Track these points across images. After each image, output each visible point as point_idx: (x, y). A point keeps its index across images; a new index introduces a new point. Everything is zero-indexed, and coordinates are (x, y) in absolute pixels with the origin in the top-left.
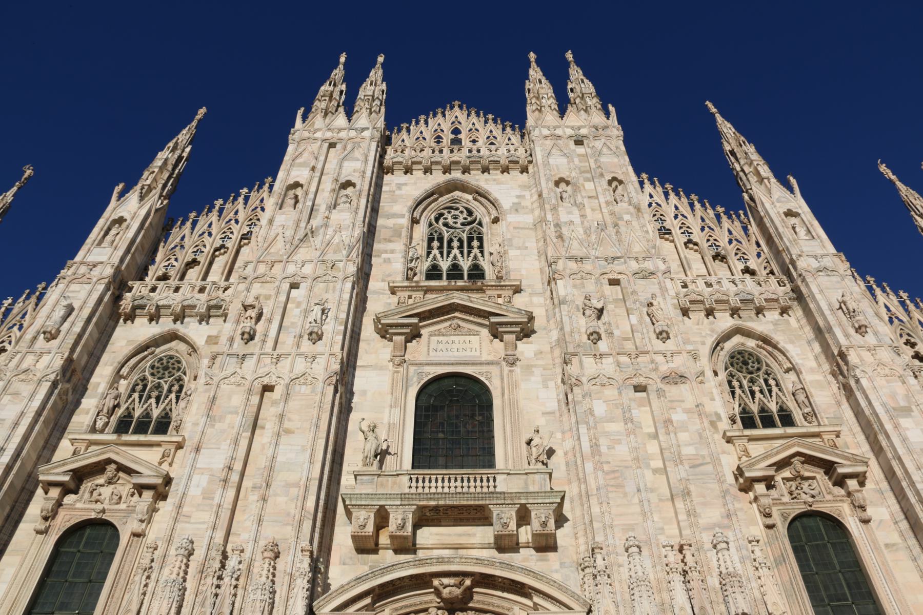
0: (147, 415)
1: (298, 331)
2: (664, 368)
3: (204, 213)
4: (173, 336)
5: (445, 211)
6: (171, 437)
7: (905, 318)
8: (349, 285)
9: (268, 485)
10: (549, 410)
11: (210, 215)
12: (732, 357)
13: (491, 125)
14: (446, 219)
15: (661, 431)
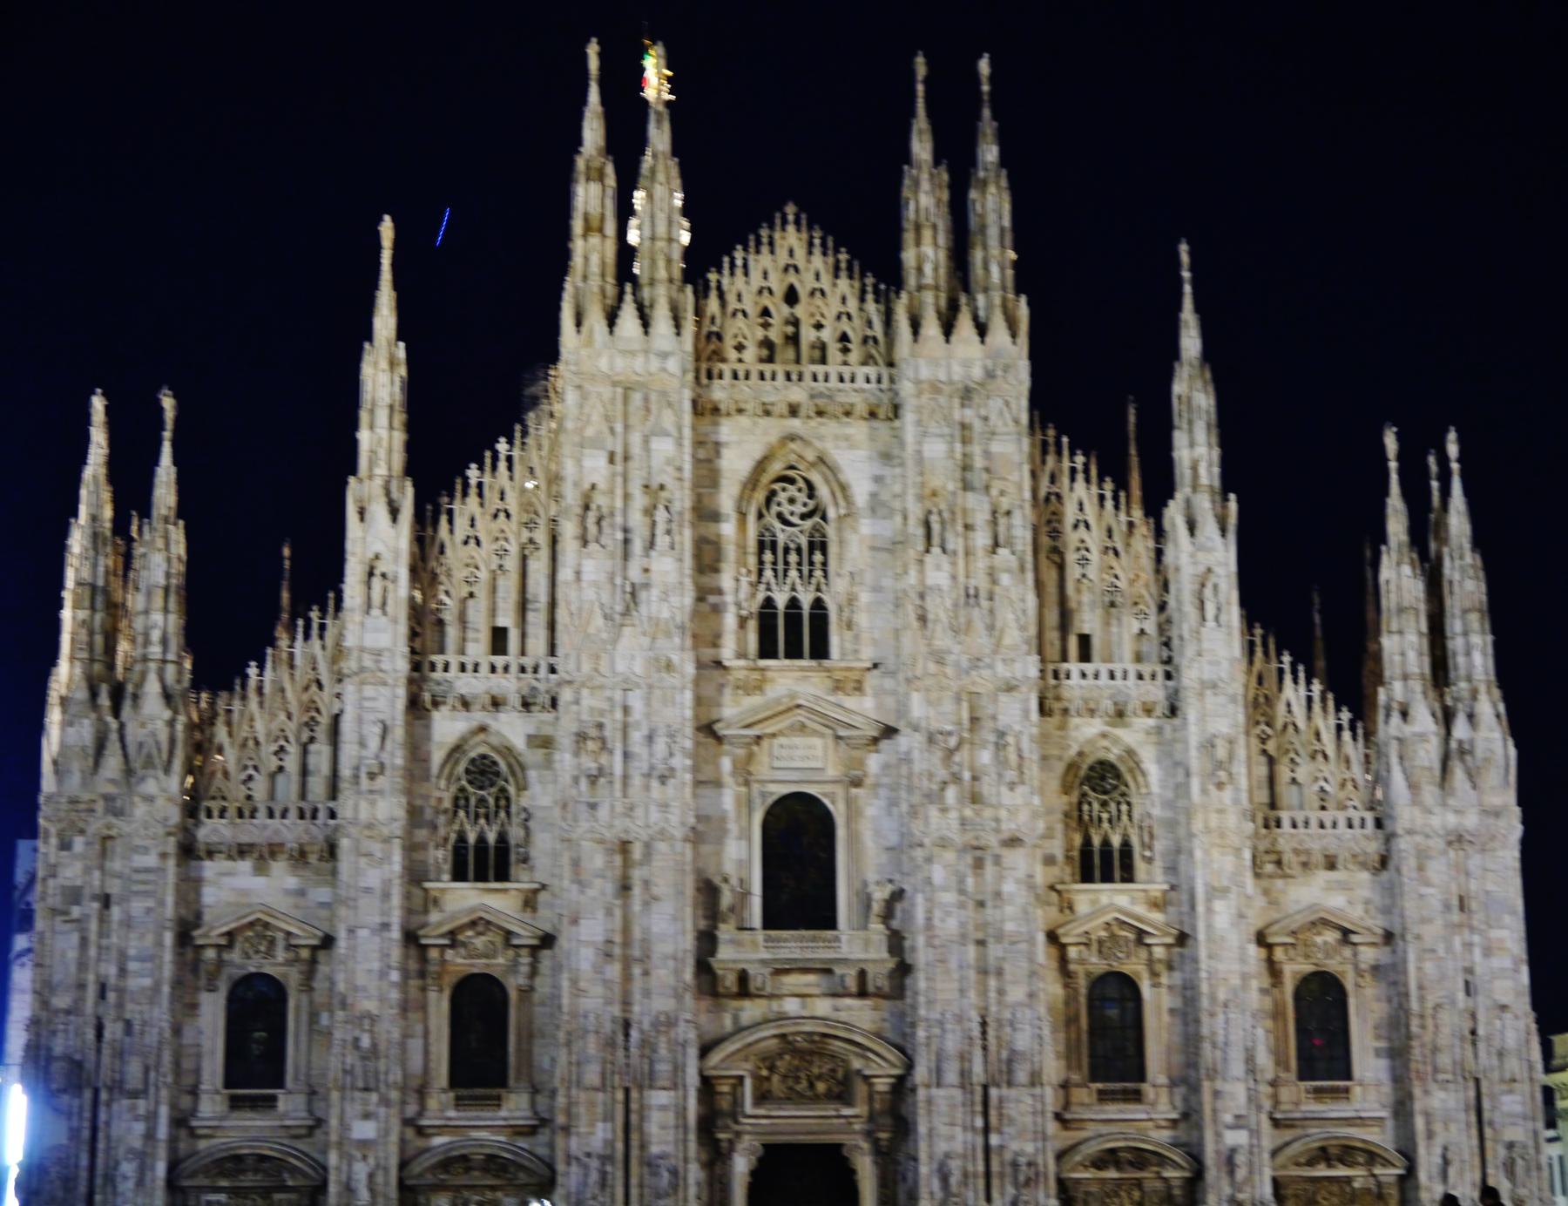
0: (481, 840)
1: (645, 767)
2: (1009, 827)
3: (458, 494)
4: (483, 729)
5: (777, 486)
6: (522, 881)
7: (1301, 723)
8: (688, 696)
9: (645, 958)
10: (890, 844)
11: (468, 500)
12: (1091, 768)
13: (844, 284)
14: (779, 504)
15: (989, 904)
